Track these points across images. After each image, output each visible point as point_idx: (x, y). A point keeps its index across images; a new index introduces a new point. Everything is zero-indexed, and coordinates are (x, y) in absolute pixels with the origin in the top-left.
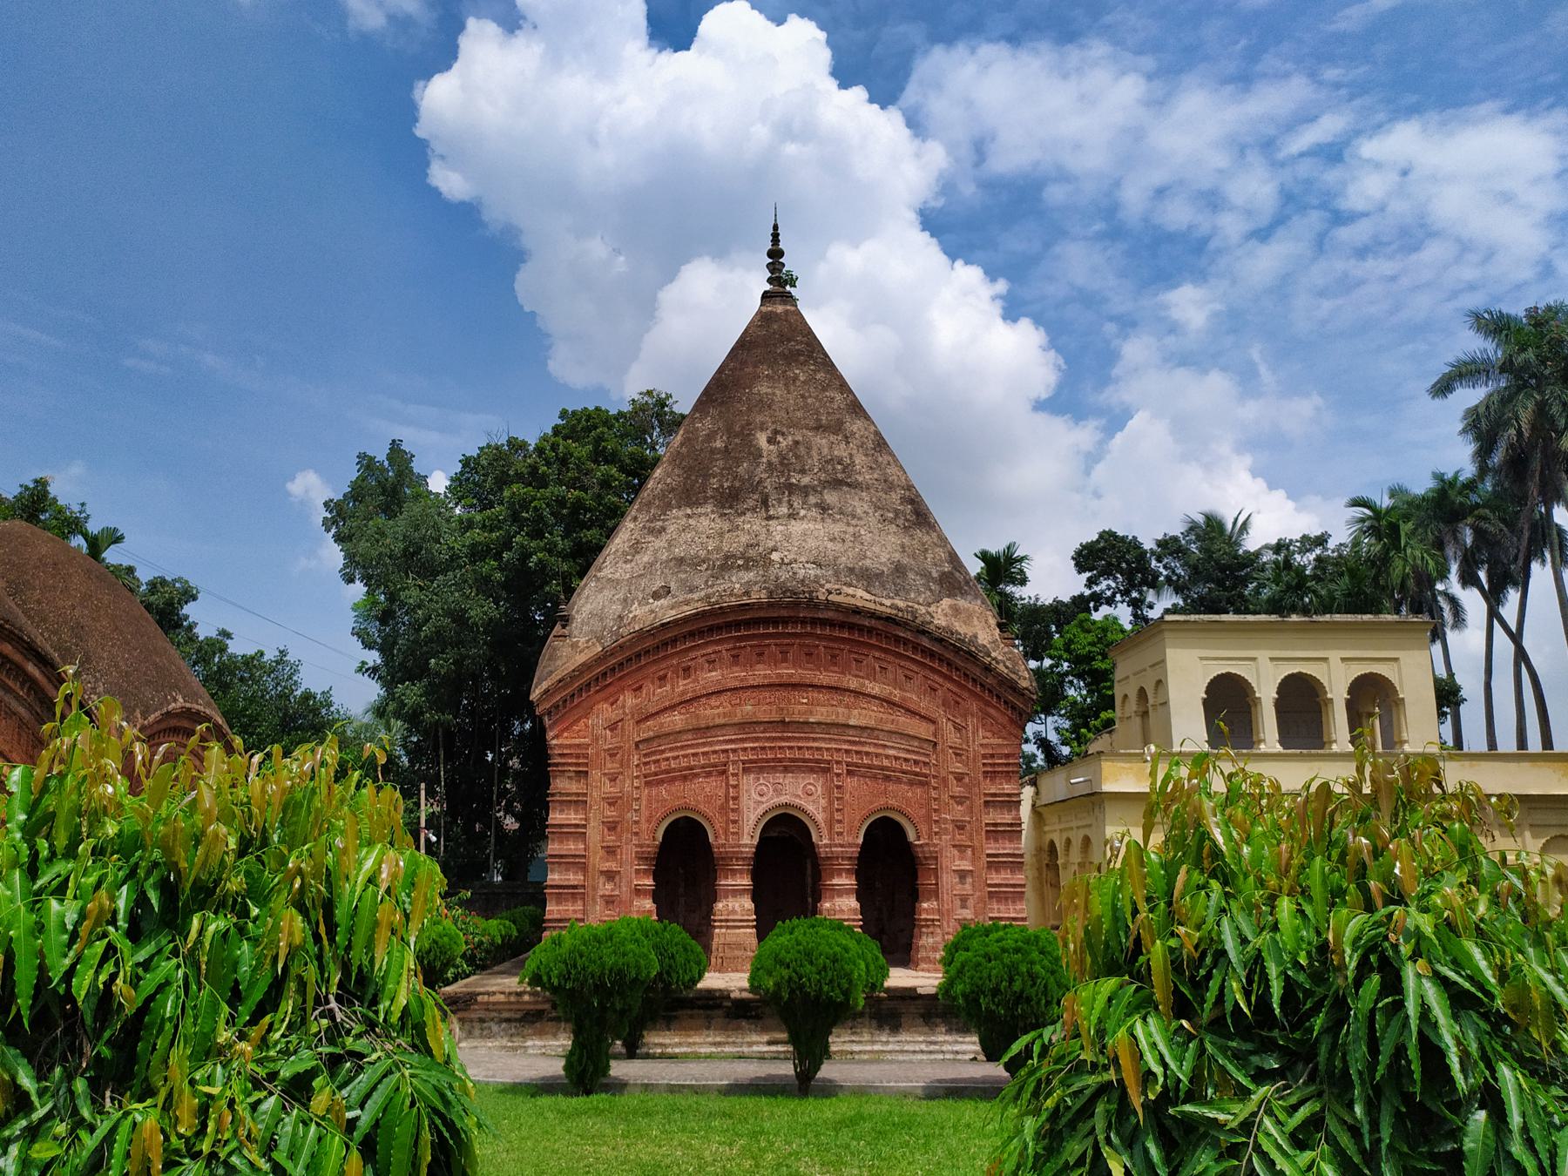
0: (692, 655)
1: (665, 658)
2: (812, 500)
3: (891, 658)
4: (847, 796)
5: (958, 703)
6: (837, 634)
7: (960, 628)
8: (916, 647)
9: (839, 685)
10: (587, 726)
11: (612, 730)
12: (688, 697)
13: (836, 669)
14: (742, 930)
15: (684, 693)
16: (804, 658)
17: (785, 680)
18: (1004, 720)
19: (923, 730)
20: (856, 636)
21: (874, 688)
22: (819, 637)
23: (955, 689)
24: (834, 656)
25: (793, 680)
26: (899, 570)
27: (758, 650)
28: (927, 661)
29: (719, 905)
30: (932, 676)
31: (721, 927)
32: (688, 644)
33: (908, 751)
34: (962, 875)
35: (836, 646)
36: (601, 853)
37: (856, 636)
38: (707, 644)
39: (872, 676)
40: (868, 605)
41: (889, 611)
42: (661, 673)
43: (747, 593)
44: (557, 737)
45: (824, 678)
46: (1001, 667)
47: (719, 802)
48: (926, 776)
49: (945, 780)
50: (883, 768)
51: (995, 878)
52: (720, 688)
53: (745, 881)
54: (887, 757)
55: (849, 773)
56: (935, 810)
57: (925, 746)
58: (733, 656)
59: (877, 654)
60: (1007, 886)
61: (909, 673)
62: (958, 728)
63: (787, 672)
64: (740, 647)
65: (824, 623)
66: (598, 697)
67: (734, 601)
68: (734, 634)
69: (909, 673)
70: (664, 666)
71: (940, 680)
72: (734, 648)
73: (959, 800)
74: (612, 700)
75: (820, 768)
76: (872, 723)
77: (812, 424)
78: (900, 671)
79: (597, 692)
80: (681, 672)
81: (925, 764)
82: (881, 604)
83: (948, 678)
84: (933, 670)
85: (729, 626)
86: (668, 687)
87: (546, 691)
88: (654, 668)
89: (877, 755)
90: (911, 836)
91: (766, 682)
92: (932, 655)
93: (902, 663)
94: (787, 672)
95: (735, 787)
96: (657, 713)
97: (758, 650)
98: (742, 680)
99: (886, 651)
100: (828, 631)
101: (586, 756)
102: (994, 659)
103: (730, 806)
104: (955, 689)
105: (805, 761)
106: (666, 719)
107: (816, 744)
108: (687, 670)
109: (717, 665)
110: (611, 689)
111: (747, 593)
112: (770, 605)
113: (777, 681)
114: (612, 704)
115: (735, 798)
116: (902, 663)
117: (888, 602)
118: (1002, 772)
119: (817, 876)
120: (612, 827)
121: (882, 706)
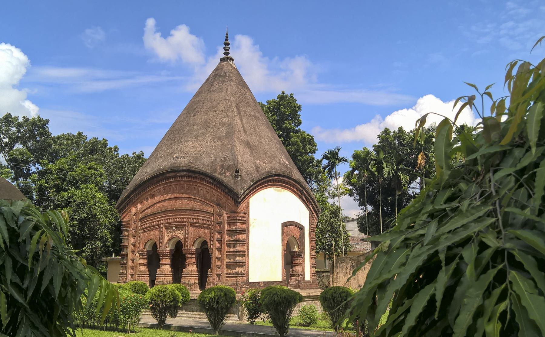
3: (203, 186)
4: (189, 233)
11: (135, 216)
14: (167, 277)
15: (151, 203)
22: (184, 181)
23: (219, 195)
24: (189, 187)
27: (169, 187)
30: (213, 191)
33: (207, 217)
44: (123, 219)
53: (168, 261)
64: (165, 187)
72: (164, 187)
78: (205, 190)
79: (132, 204)
80: (151, 196)
83: (217, 191)
89: (198, 219)
93: (206, 187)
96: (145, 210)
97: (169, 187)
99: (201, 184)
103: (161, 238)
104: (219, 195)
107: (183, 216)
108: (153, 195)
110: (135, 203)
115: (162, 236)
116: (206, 187)
120: (134, 245)
121: (200, 203)
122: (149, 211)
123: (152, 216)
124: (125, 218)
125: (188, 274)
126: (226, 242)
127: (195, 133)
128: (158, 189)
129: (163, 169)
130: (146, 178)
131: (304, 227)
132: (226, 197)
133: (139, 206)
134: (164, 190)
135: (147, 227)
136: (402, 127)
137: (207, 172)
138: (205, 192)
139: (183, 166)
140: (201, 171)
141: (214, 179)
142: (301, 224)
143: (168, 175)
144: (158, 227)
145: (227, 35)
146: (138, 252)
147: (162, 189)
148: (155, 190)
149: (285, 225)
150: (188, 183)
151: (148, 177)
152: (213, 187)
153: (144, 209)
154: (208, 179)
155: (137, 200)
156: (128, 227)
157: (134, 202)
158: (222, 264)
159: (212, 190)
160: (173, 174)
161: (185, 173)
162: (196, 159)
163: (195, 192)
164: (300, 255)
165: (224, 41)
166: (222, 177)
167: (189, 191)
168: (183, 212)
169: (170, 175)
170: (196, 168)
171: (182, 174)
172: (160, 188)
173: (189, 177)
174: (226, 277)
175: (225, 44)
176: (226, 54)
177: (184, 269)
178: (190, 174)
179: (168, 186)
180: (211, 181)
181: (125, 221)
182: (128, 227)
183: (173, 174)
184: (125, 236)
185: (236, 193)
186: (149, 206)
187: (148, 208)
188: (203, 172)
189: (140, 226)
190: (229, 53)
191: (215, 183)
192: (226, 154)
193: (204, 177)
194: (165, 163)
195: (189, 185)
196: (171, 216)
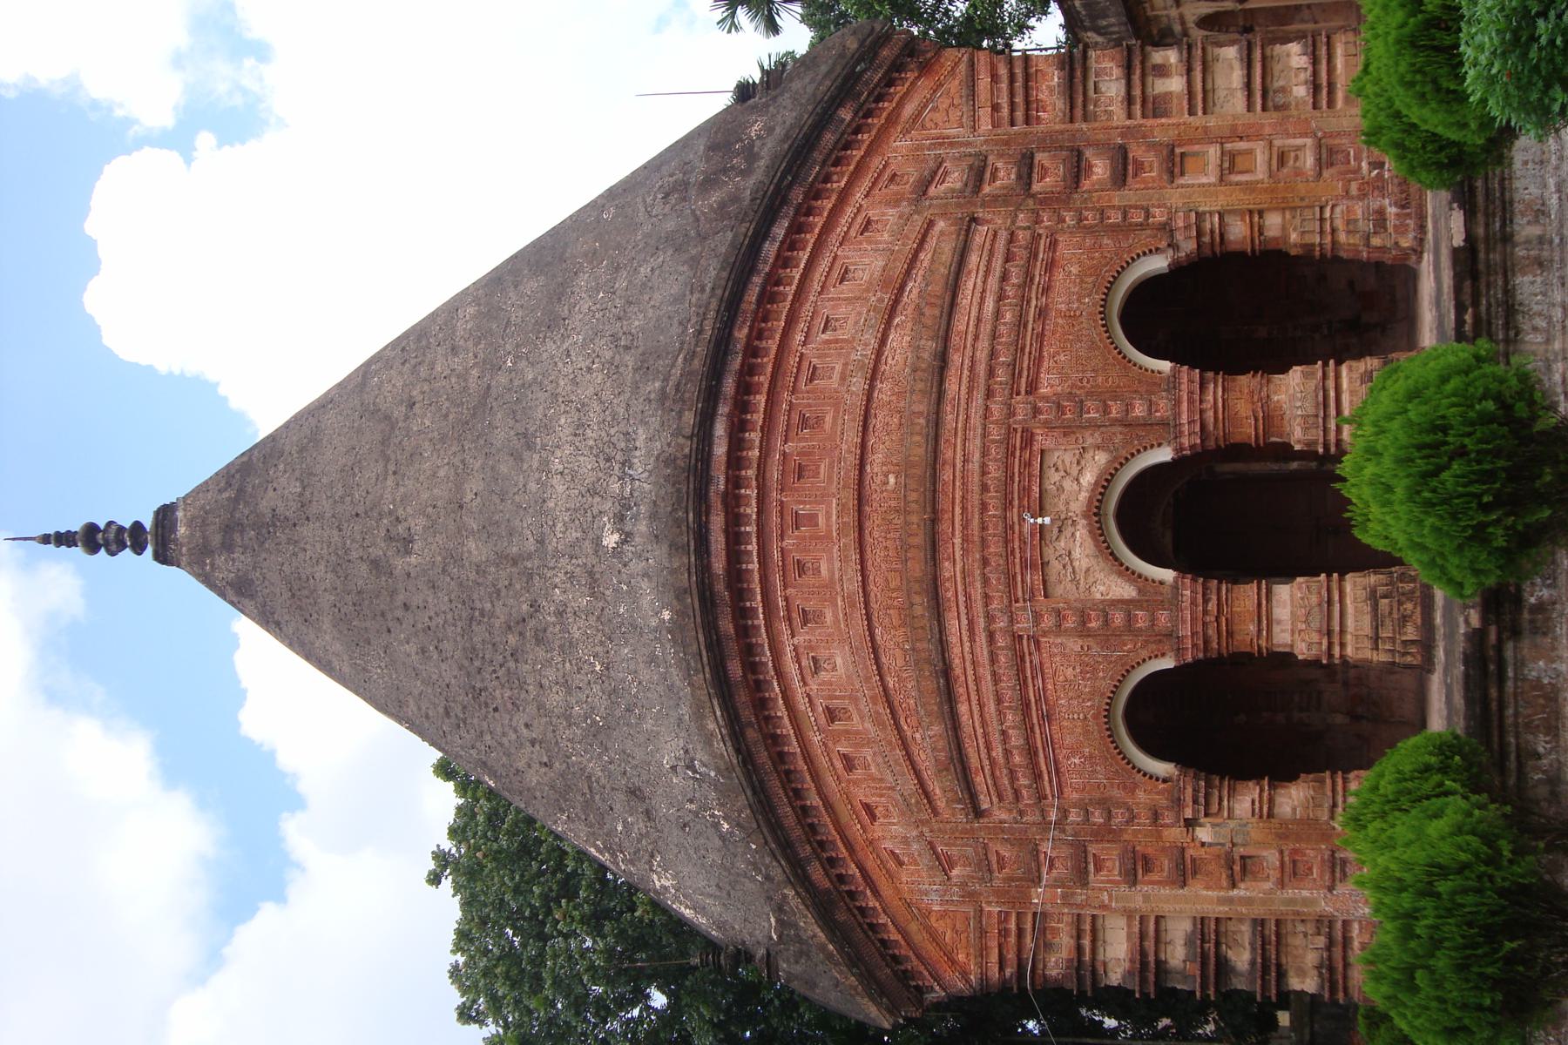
0: (802, 703)
1: (808, 758)
5: (894, 176)
6: (758, 418)
8: (783, 261)
9: (860, 412)
10: (943, 915)
11: (951, 868)
12: (885, 712)
15: (877, 721)
16: (807, 483)
17: (850, 518)
18: (924, 86)
20: (763, 379)
24: (804, 422)
28: (811, 238)
29: (1302, 651)
30: (840, 230)
31: (1342, 645)
32: (781, 711)
35: (782, 419)
37: (763, 379)
38: (780, 674)
42: (839, 765)
44: (965, 975)
47: (1096, 649)
52: (866, 652)
53: (1247, 595)
54: (998, 314)
55: (1032, 388)
57: (978, 240)
58: (805, 623)
59: (799, 337)
61: (835, 274)
63: (830, 515)
64: (788, 609)
66: (886, 890)
68: (760, 620)
69: (835, 274)
70: (823, 762)
71: (849, 211)
72: (790, 619)
74: (892, 865)
78: (833, 292)
79: (876, 893)
80: (837, 725)
81: (1012, 238)
83: (844, 196)
84: (827, 228)
86: (868, 753)
88: (830, 781)
90: (1158, 264)
91: (855, 557)
92: (797, 228)
93: (816, 287)
96: (917, 774)
98: (852, 605)
100: (754, 436)
101: (1003, 918)
104: (866, 183)
106: (925, 760)
109: (823, 653)
110: (871, 864)
113: (852, 536)
114: (901, 864)
116: (816, 287)
118: (1027, 89)
119: (1237, 451)
122: (927, 739)
123: (963, 708)
124: (961, 957)
125: (1325, 391)
127: (503, 469)
129: (680, 594)
130: (719, 746)
134: (806, 618)
135: (1031, 752)
137: (732, 244)
139: (678, 432)
140: (719, 292)
141: (770, 206)
143: (719, 565)
145: (45, 539)
146: (1190, 824)
150: (781, 427)
151: (712, 726)
152: (819, 221)
153: (910, 784)
154: (770, 249)
157: (862, 869)
158: (1258, 137)
159: (834, 239)
160: (717, 522)
161: (720, 429)
162: (644, 368)
166: (767, 151)
167: (828, 419)
168: (949, 454)
169: (718, 541)
170: (700, 332)
171: (720, 450)
173: (742, 406)
174: (1331, 103)
176: (135, 538)
178: (729, 385)
179: (785, 587)
180: (780, 230)
181: (983, 952)
183: (717, 522)
184: (1079, 949)
185: (862, 44)
186: (893, 736)
187: (905, 745)
188: (725, 274)
189: (1021, 813)
190: (138, 526)
191: (797, 195)
192: (649, 200)
193: (757, 280)
194: (648, 595)
195: (795, 417)
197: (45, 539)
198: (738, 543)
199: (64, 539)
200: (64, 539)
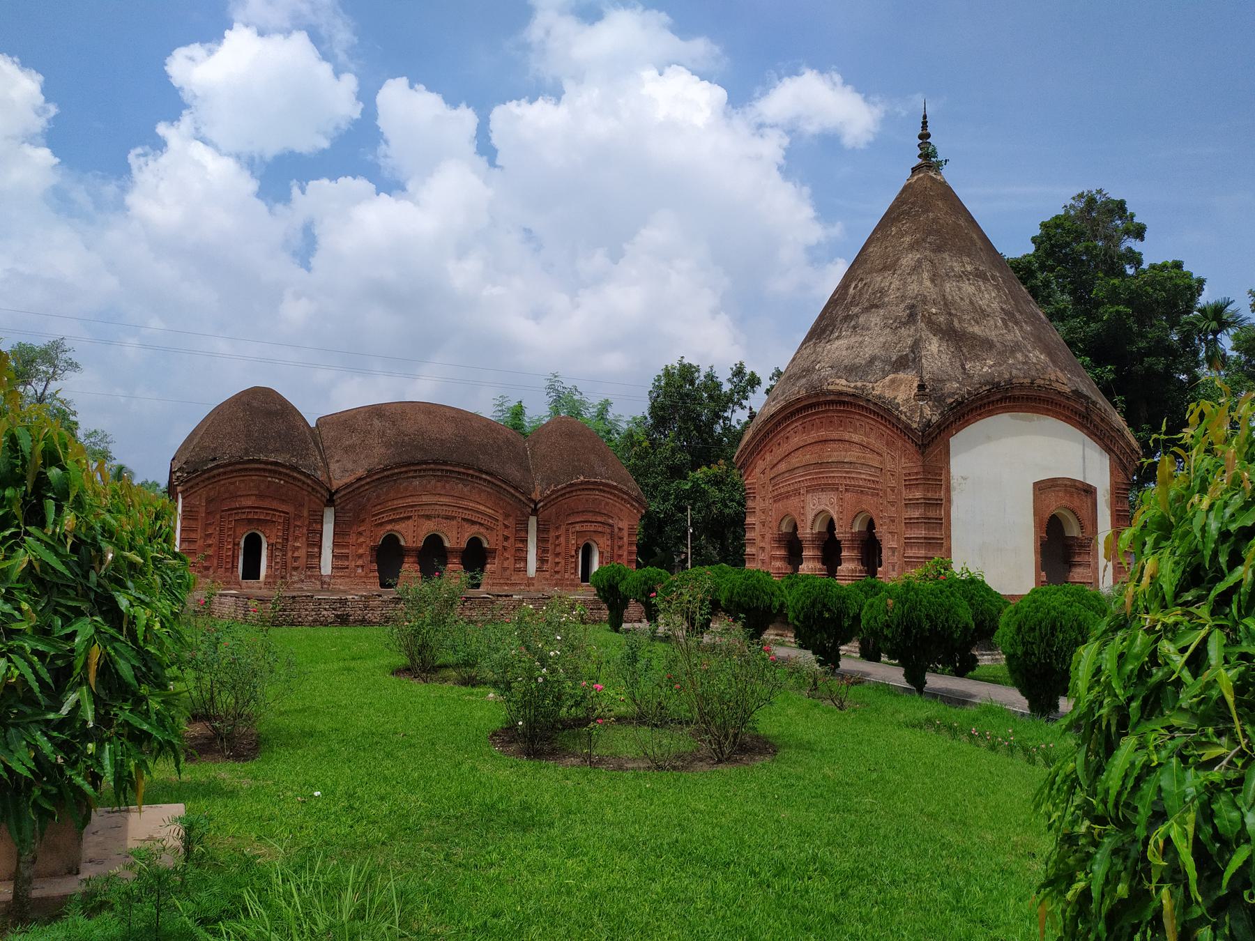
2: (853, 323)
3: (863, 418)
7: (888, 394)
13: (841, 429)
17: (821, 439)
19: (874, 461)
21: (856, 438)
25: (824, 439)
26: (872, 360)
34: (893, 550)
36: (760, 538)
38: (792, 422)
39: (855, 432)
40: (845, 389)
41: (852, 390)
43: (799, 392)
44: (746, 479)
45: (835, 435)
46: (903, 417)
48: (877, 489)
49: (885, 492)
50: (860, 486)
51: (910, 553)
56: (881, 511)
59: (857, 417)
60: (915, 557)
62: (893, 458)
63: (823, 433)
65: (832, 402)
67: (793, 398)
73: (892, 504)
75: (834, 488)
76: (854, 460)
77: (880, 267)
79: (757, 454)
82: (849, 387)
85: (799, 411)
87: (738, 457)
89: (857, 479)
91: (813, 441)
94: (823, 433)
95: (803, 501)
96: (777, 463)
102: (901, 412)
105: (829, 484)
108: (787, 438)
111: (799, 392)
112: (808, 397)
115: (803, 508)
116: (868, 421)
117: (852, 385)
123: (787, 475)
126: (904, 521)
128: (794, 426)
131: (1095, 489)
132: (901, 438)
133: (768, 457)
134: (804, 428)
135: (781, 494)
136: (610, 404)
138: (868, 430)
142: (955, 496)
144: (797, 492)
145: (925, 117)
147: (800, 428)
148: (790, 429)
149: (1042, 488)
150: (840, 415)
152: (879, 419)
153: (775, 462)
155: (765, 446)
156: (754, 493)
157: (761, 450)
159: (878, 424)
163: (852, 430)
164: (1086, 545)
165: (920, 131)
172: (796, 424)
175: (921, 137)
177: (839, 567)
182: (754, 493)
186: (783, 455)
196: (816, 473)
197: (925, 117)
198: (805, 409)
199: (925, 124)
200: (925, 124)
